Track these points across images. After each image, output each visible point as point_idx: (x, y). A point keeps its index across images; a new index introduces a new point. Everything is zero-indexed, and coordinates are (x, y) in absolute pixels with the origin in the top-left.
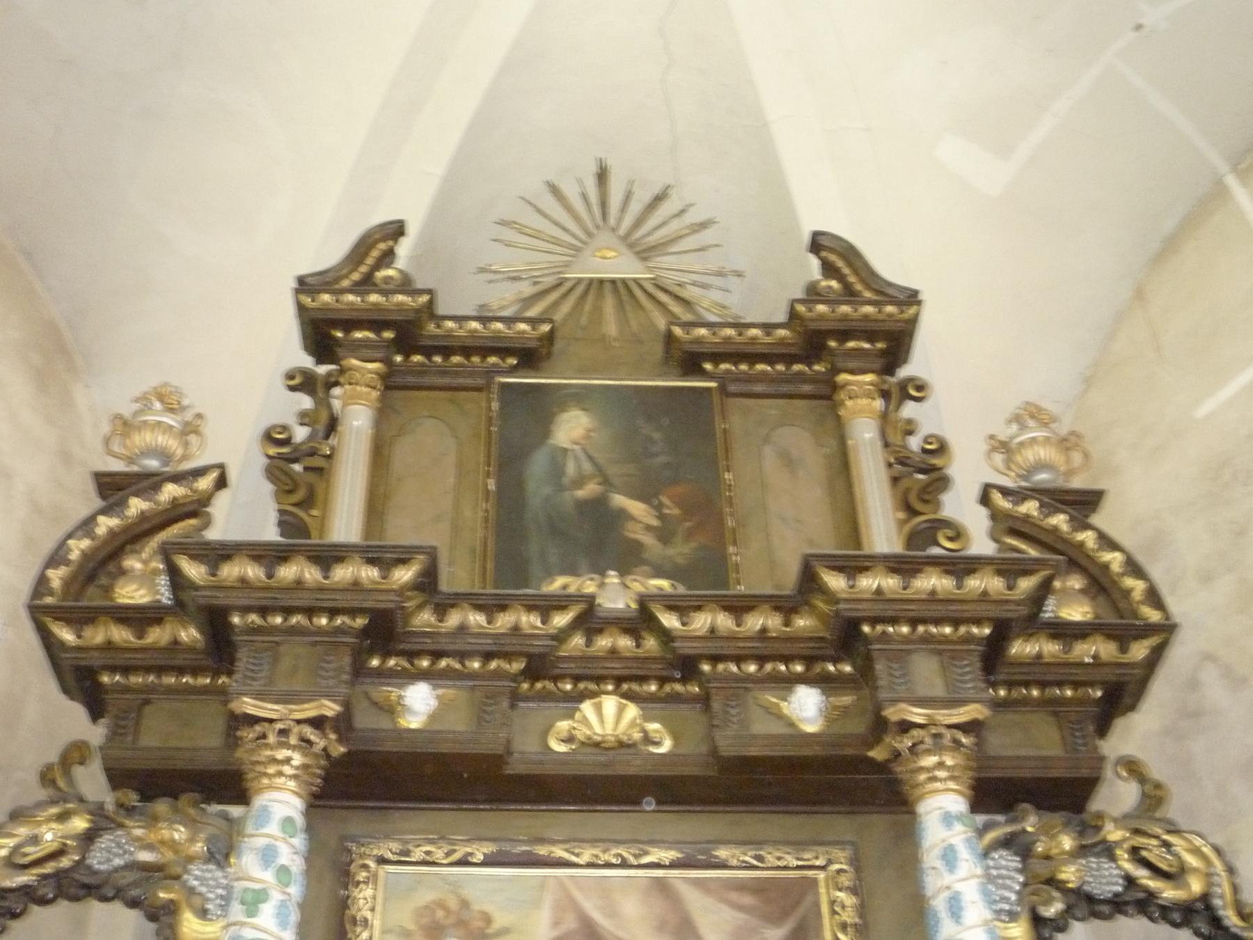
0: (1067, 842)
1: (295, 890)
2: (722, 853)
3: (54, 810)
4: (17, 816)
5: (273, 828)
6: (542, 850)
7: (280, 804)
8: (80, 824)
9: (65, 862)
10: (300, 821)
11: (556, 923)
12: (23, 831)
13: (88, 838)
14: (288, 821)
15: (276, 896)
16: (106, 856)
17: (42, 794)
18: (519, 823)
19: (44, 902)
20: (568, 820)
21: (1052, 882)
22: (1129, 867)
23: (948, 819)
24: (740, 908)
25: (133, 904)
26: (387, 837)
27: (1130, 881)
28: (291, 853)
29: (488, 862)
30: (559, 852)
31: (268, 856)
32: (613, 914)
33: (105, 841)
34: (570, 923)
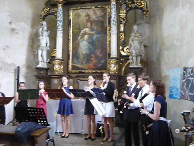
0: (130, 2)
1: (62, 16)
2: (99, 6)
3: (47, 8)
4: (44, 9)
5: (59, 11)
6: (84, 8)
7: (60, 8)
8: (49, 9)
9: (48, 12)
10: (62, 10)
11: (85, 14)
12: (45, 10)
13: (49, 10)
14: (61, 10)
15: (60, 16)
16: (51, 12)
17: (45, 6)
18: (83, 5)
19: (47, 15)
20: (85, 5)
21: (128, 7)
22: (136, 5)
23: (113, 5)
24: (100, 11)
25: (54, 15)
26: (72, 8)
27: (136, 6)
28: (61, 13)
29: (80, 9)
30: (85, 8)
31: (59, 13)
32: (90, 13)
33: (50, 10)
34: (87, 14)
